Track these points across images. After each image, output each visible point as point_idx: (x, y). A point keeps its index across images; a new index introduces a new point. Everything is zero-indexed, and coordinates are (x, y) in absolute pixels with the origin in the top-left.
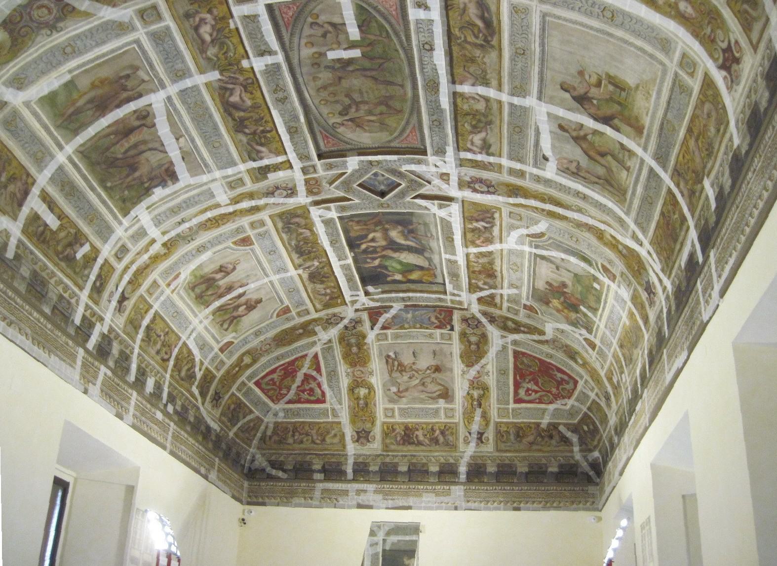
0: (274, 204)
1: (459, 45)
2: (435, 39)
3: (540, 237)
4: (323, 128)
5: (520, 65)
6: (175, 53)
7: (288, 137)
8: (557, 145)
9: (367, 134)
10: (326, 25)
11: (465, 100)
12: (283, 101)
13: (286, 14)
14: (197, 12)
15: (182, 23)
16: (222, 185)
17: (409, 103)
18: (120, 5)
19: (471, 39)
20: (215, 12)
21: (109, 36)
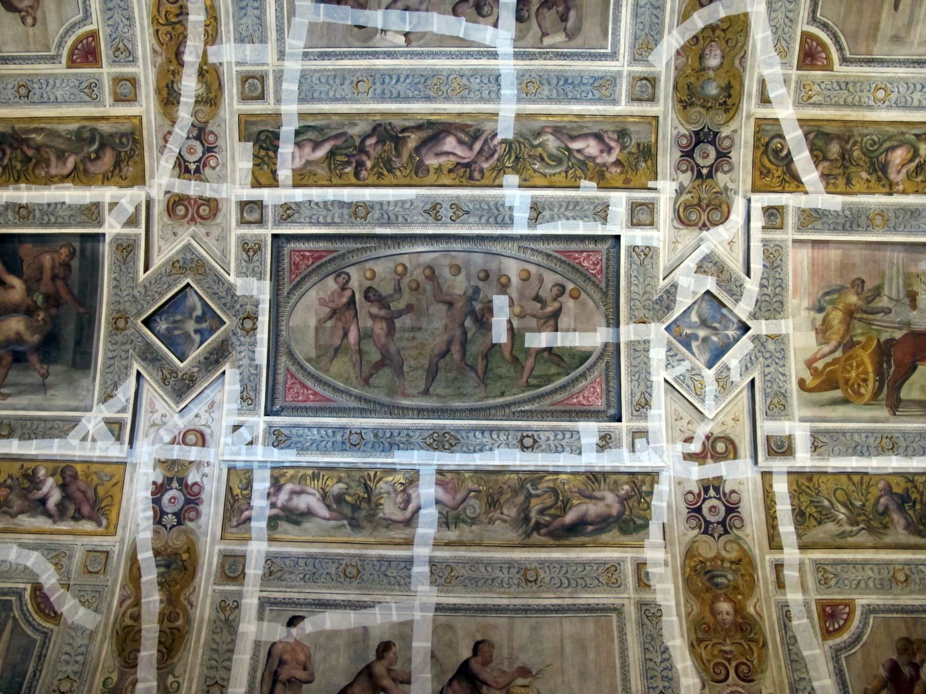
0: (170, 133)
1: (522, 486)
2: (545, 454)
3: (40, 611)
4: (343, 256)
5: (497, 573)
6: (570, 96)
7: (346, 199)
8: (340, 642)
9: (313, 323)
10: (556, 305)
11: (399, 488)
12: (433, 211)
13: (588, 256)
14: (623, 147)
15: (614, 122)
16: (263, 64)
17: (386, 400)
18: (676, 60)
19: (536, 505)
20: (616, 170)
21: (641, 26)
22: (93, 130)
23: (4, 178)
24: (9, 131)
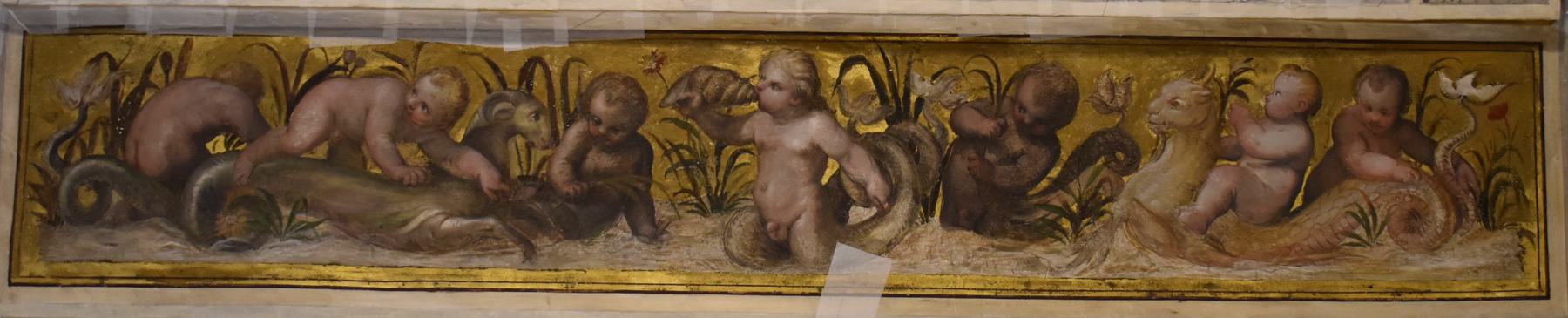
22: (205, 236)
23: (588, 74)
24: (543, 243)
